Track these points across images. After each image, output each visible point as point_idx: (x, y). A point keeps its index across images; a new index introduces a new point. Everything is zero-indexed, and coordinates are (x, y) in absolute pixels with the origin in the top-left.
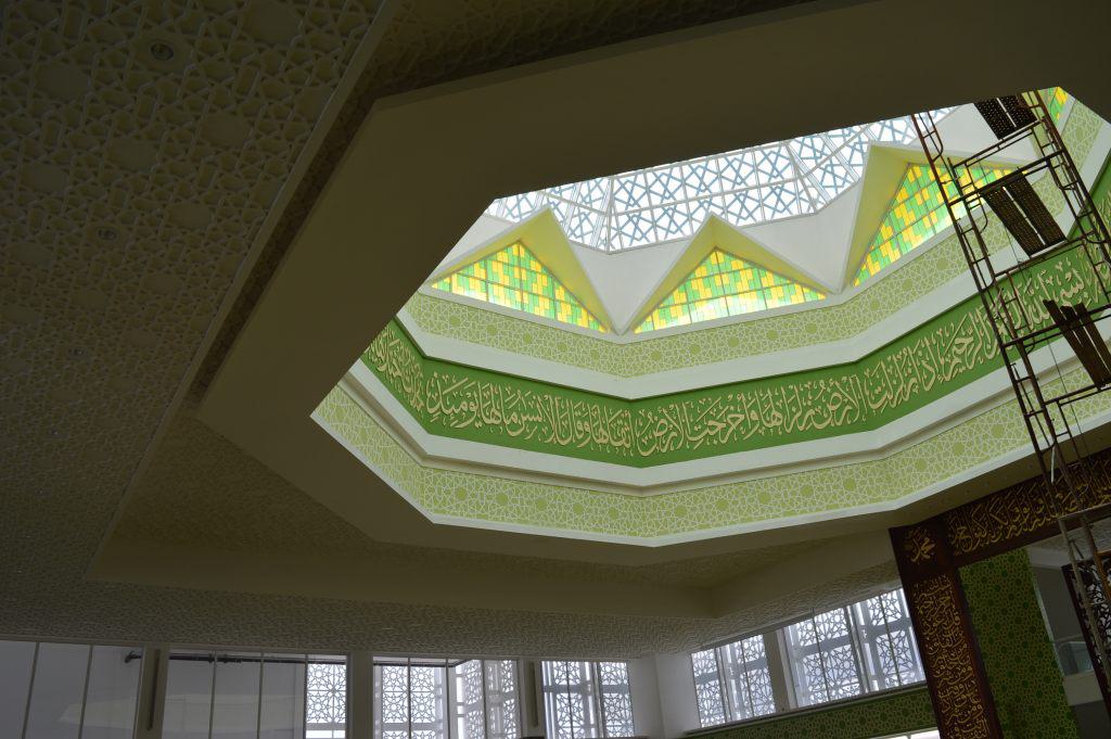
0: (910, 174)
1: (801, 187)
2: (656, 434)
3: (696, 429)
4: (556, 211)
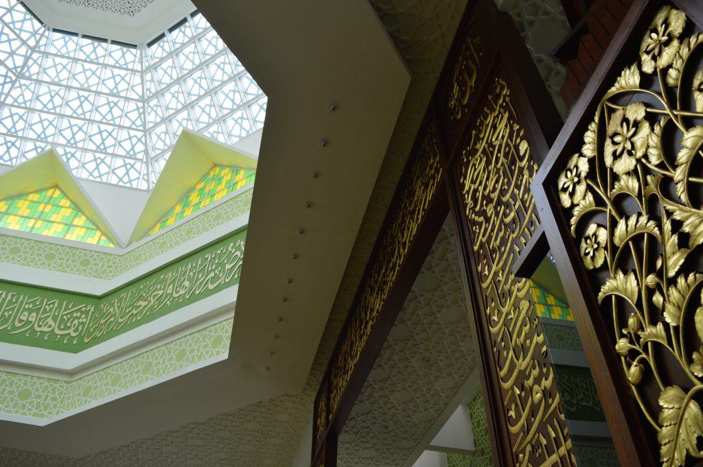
0: (51, 192)
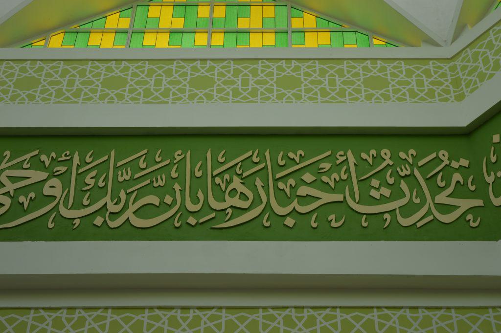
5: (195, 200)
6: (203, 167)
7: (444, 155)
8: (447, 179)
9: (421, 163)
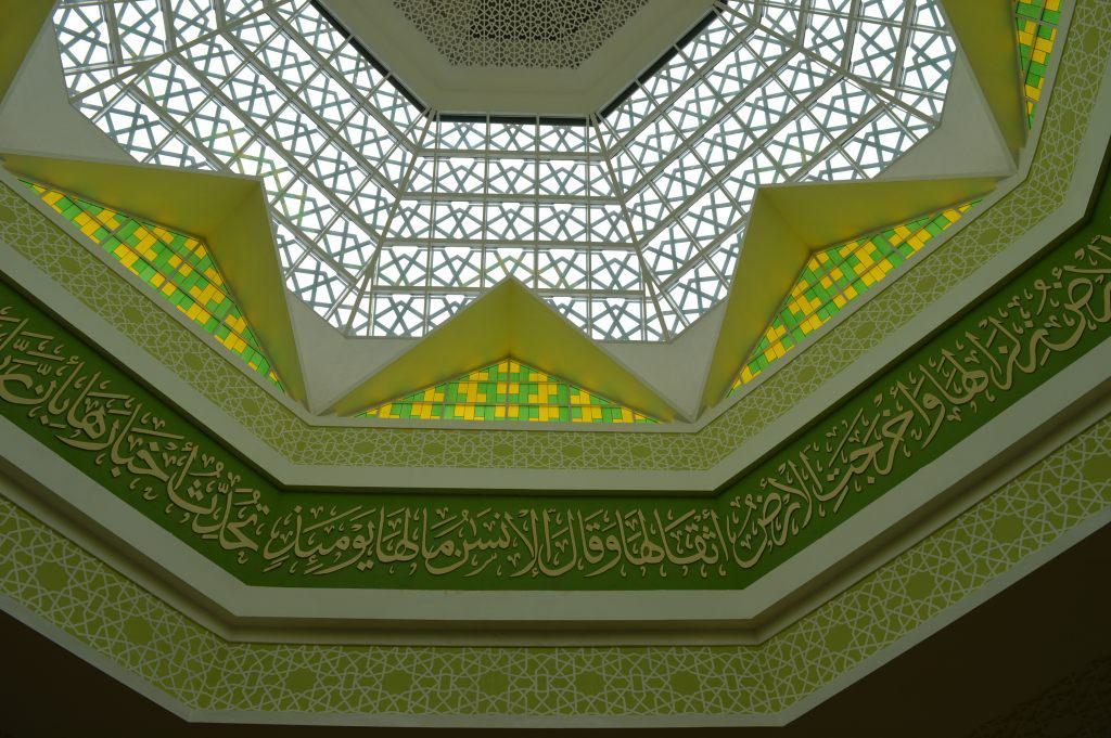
1: (901, 114)
2: (762, 523)
3: (830, 478)
4: (570, 317)
5: (59, 405)
6: (85, 384)
7: (257, 495)
8: (247, 514)
9: (237, 491)
